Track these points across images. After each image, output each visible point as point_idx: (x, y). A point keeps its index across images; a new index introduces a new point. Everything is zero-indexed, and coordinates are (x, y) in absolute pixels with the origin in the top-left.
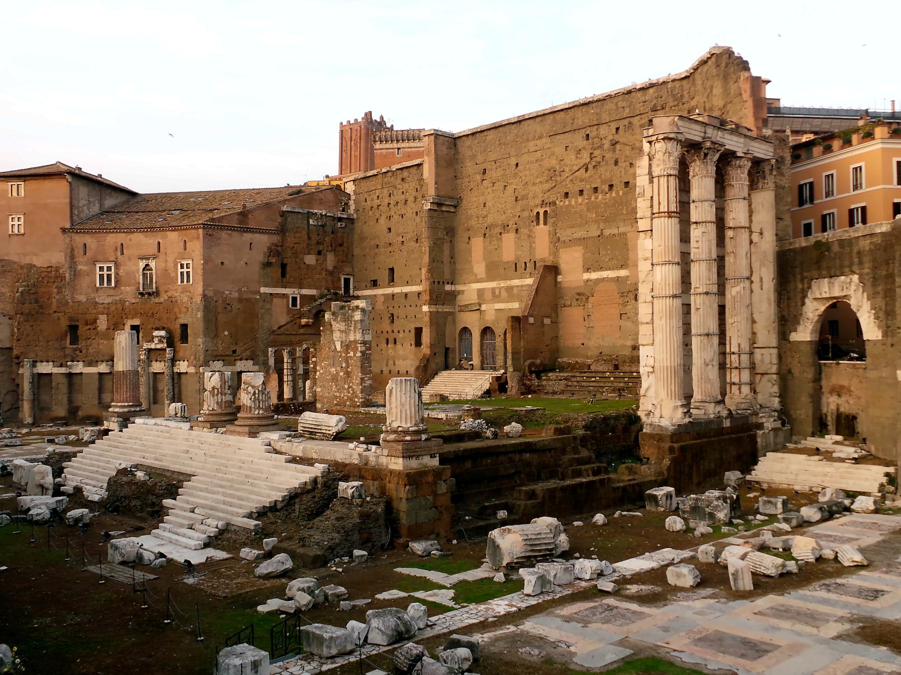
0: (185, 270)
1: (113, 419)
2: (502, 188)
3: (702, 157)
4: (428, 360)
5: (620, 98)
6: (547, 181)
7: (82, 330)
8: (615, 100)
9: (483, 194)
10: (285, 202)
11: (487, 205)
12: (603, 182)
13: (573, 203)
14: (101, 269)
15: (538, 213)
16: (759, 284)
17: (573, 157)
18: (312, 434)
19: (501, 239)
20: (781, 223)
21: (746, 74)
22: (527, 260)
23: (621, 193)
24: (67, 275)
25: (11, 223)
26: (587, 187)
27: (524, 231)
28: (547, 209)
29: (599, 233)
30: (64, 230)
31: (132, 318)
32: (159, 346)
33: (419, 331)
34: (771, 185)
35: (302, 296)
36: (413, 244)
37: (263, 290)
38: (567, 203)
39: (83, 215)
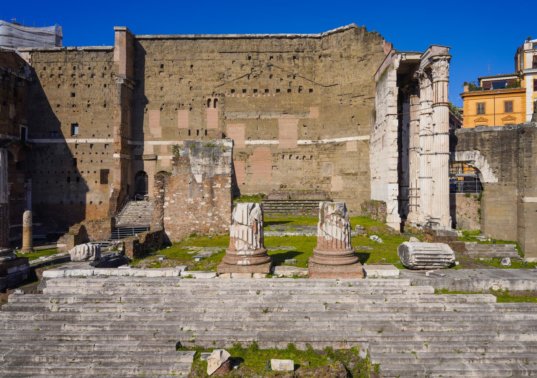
5: (274, 39)
6: (217, 80)
8: (270, 40)
9: (161, 81)
11: (164, 89)
12: (261, 87)
16: (406, 153)
17: (239, 68)
19: (177, 113)
23: (274, 95)
26: (249, 89)
28: (217, 97)
29: (257, 117)
36: (101, 108)
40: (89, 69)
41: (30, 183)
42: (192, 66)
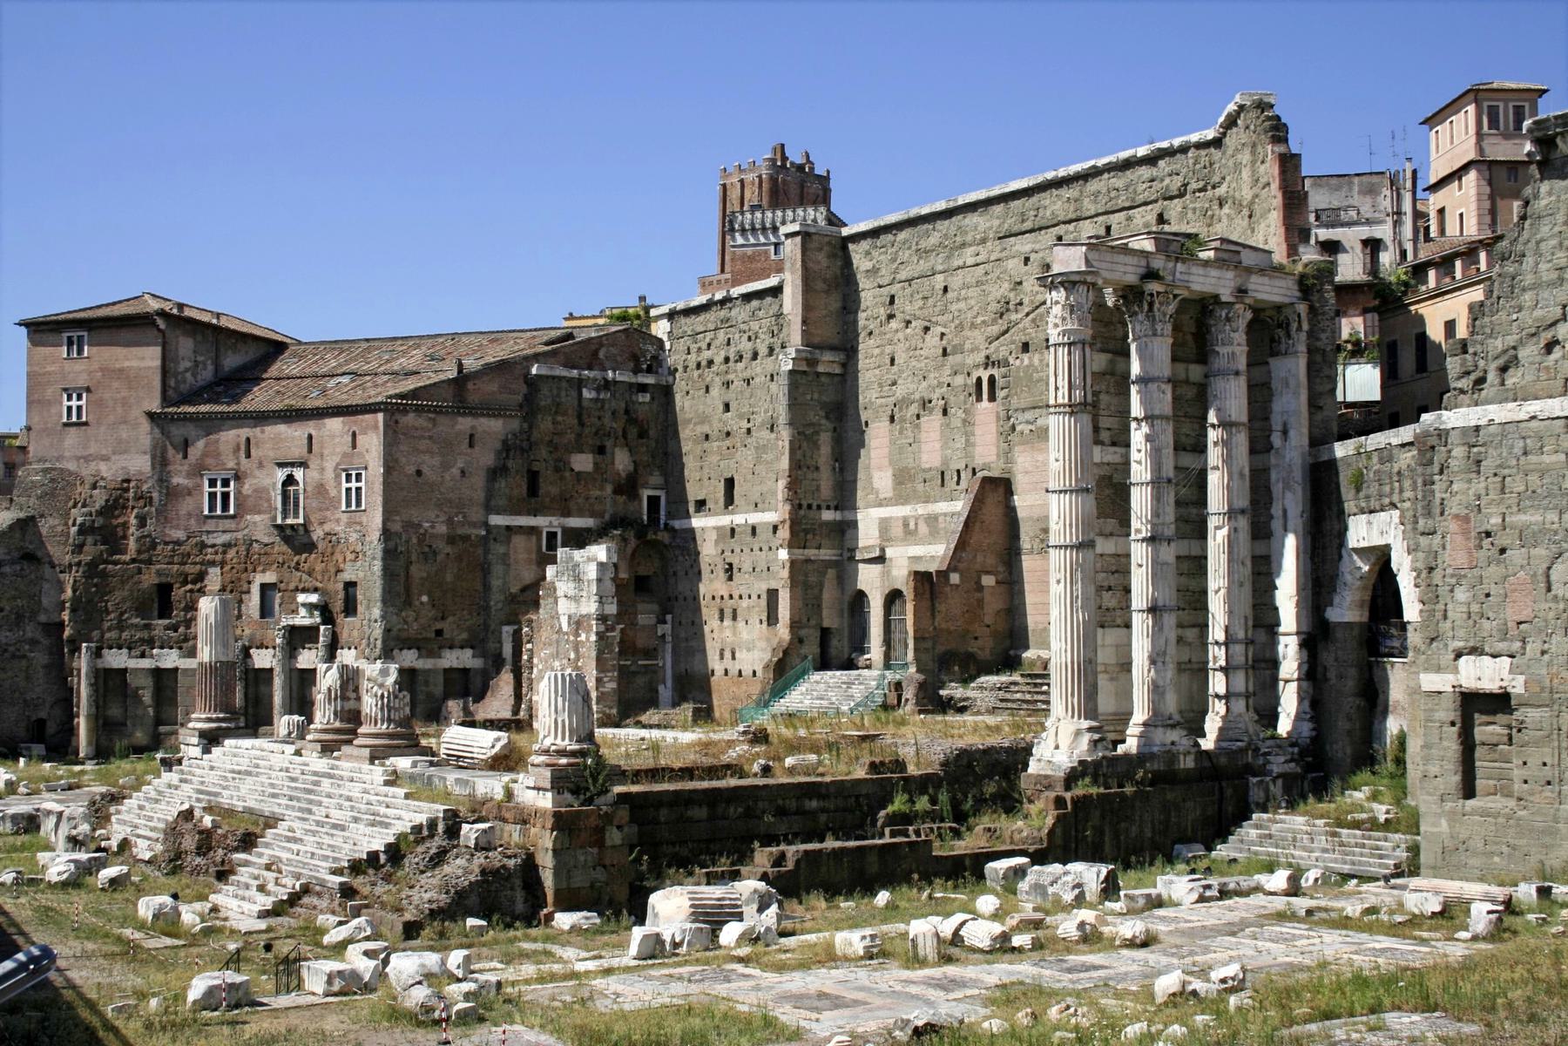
0: (354, 485)
2: (919, 331)
3: (1146, 307)
4: (785, 652)
6: (994, 322)
7: (178, 593)
10: (536, 357)
13: (1036, 362)
14: (213, 483)
15: (979, 380)
18: (458, 761)
19: (918, 426)
20: (1319, 417)
21: (1281, 149)
22: (961, 466)
24: (155, 495)
25: (66, 403)
27: (957, 414)
30: (151, 416)
31: (263, 571)
32: (307, 622)
33: (772, 595)
34: (1302, 348)
35: (566, 531)
36: (765, 434)
37: (497, 520)
38: (1026, 362)
39: (184, 388)
40: (749, 339)
41: (668, 627)
42: (946, 289)
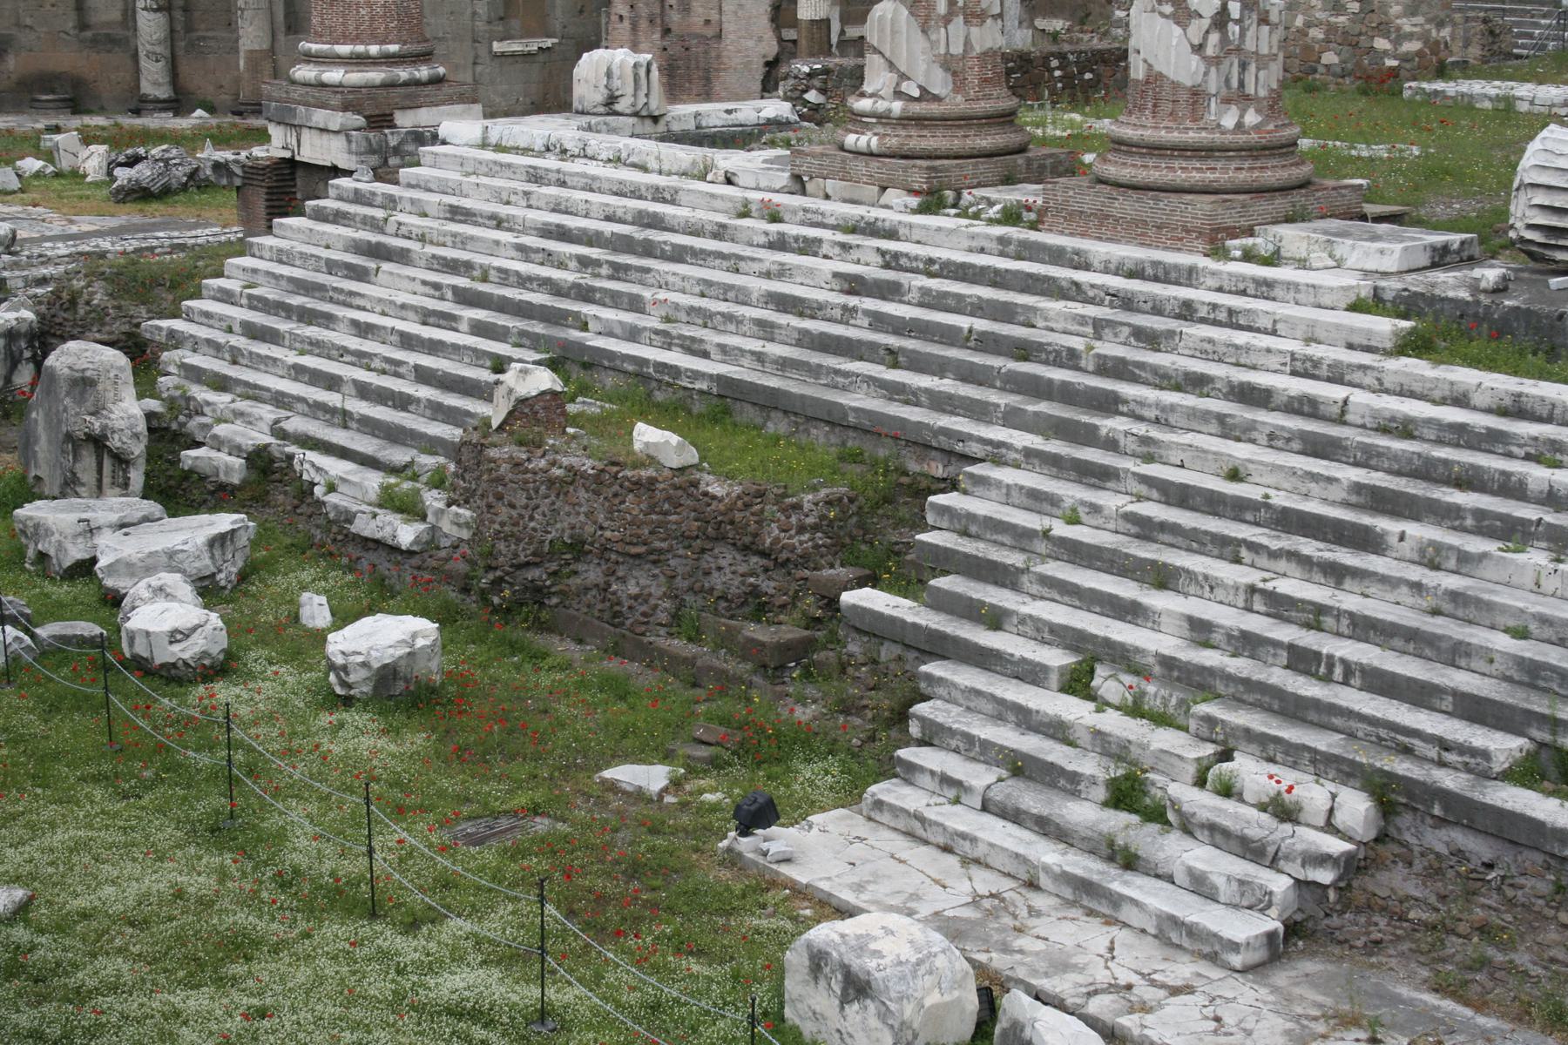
1: (320, 117)
